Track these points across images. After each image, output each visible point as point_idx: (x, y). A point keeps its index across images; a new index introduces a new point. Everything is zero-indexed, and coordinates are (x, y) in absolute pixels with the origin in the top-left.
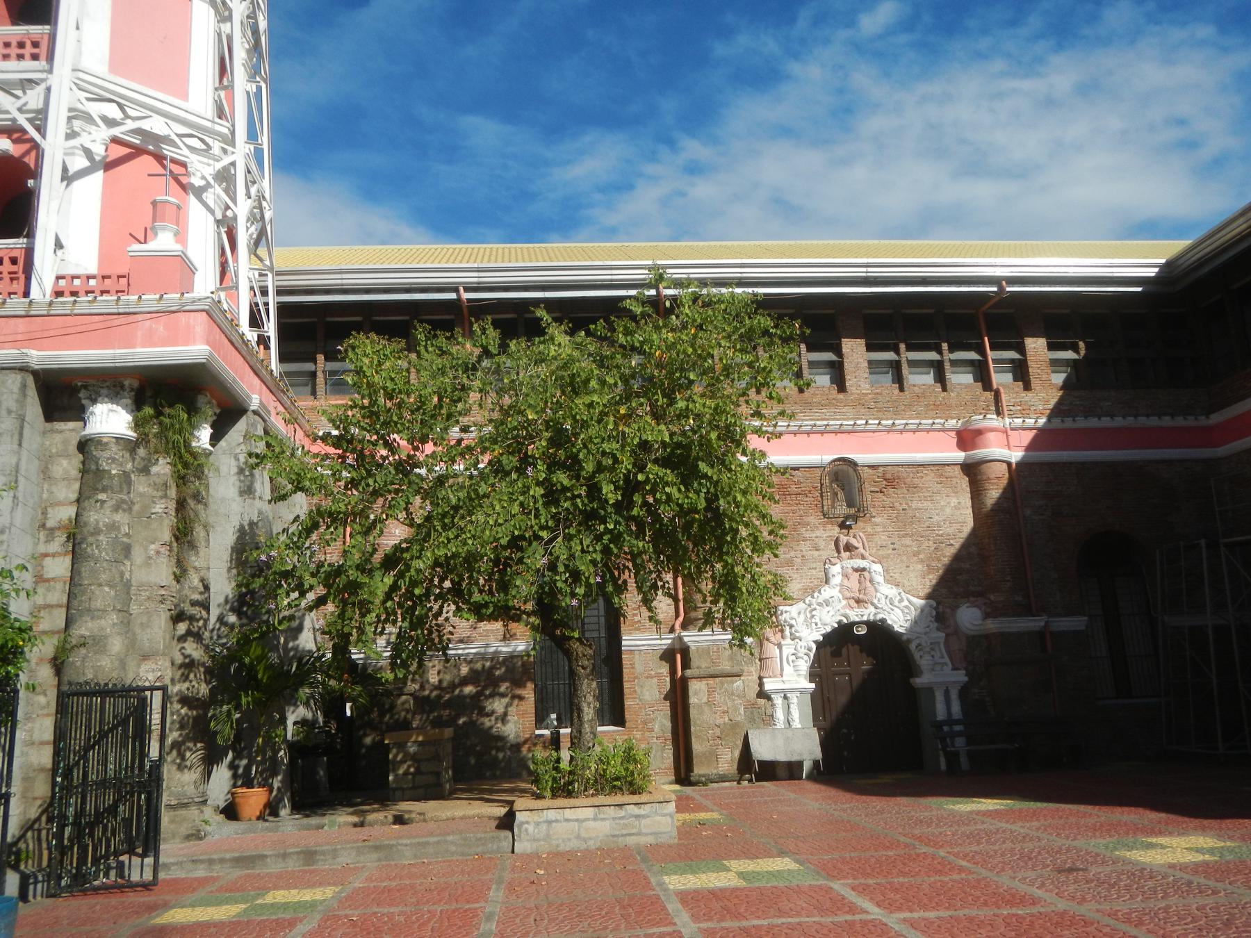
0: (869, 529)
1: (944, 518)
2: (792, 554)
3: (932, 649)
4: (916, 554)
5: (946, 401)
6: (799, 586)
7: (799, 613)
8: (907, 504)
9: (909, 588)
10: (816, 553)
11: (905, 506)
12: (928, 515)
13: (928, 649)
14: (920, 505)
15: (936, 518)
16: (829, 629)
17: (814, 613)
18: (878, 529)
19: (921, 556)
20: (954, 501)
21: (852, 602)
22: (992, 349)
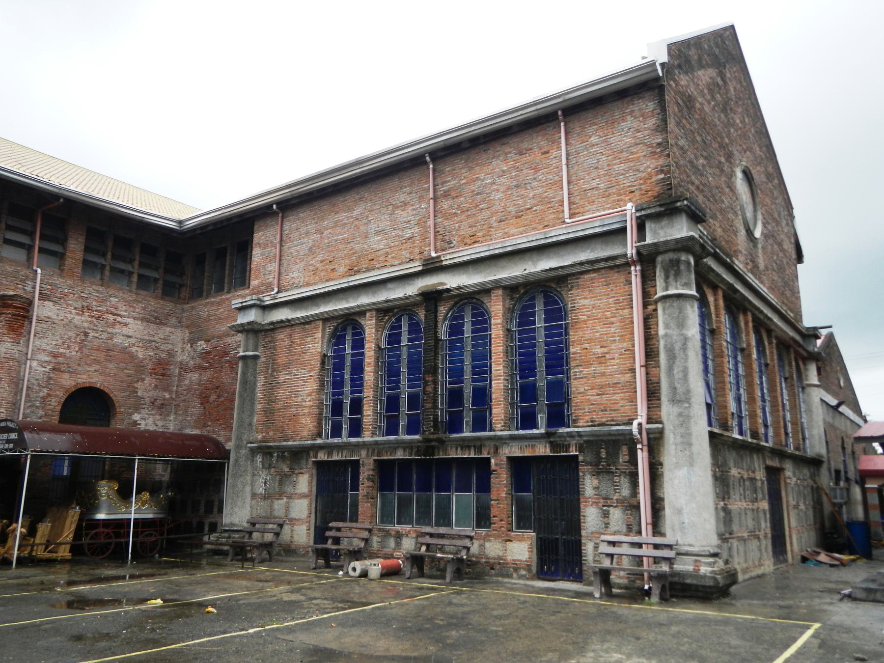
22: (41, 238)
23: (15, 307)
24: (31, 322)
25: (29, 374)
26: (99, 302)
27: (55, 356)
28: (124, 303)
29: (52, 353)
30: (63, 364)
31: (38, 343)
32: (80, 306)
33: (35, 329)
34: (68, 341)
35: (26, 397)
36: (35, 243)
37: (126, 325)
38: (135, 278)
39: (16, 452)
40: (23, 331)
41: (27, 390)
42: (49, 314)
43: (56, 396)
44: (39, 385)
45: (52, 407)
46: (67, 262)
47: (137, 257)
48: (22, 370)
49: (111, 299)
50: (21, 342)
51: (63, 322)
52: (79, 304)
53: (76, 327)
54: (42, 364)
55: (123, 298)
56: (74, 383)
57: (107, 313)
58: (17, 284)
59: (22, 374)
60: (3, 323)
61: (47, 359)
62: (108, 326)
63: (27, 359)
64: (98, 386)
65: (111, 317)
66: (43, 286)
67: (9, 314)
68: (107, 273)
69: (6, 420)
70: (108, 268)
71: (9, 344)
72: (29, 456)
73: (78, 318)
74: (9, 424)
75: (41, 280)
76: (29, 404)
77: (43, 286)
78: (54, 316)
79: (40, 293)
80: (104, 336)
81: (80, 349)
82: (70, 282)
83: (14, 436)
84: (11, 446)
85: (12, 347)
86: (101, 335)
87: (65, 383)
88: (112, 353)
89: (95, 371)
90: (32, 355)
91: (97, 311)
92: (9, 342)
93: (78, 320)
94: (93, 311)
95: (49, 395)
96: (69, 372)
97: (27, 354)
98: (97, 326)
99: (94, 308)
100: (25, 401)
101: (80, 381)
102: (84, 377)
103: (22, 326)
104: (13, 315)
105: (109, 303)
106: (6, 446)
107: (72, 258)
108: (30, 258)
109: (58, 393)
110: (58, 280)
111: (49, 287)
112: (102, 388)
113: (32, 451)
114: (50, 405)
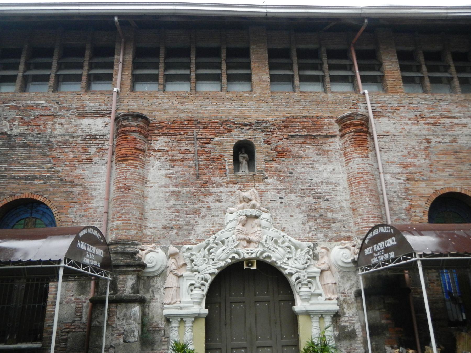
0: (262, 187)
1: (321, 180)
2: (200, 204)
3: (309, 282)
4: (299, 206)
5: (325, 99)
6: (203, 230)
7: (199, 251)
8: (293, 169)
9: (292, 233)
10: (218, 204)
11: (291, 171)
12: (309, 178)
13: (305, 282)
14: (303, 170)
15: (315, 180)
16: (222, 264)
17: (211, 251)
18: (269, 187)
19: (303, 208)
20: (330, 167)
21: (245, 243)
22: (360, 70)
23: (355, 125)
24: (373, 139)
25: (386, 188)
26: (429, 109)
27: (406, 167)
28: (455, 105)
29: (401, 164)
30: (415, 173)
31: (385, 156)
32: (413, 116)
33: (379, 144)
34: (413, 150)
35: (390, 210)
36: (356, 72)
37: (465, 125)
38: (456, 82)
39: (400, 261)
40: (368, 146)
41: (389, 204)
42: (387, 129)
43: (419, 206)
44: (399, 197)
45: (419, 218)
46: (388, 81)
47: (451, 63)
48: (378, 184)
49: (441, 103)
50: (369, 155)
51: (402, 134)
52: (412, 115)
53: (416, 135)
54: (396, 176)
55: (453, 101)
56: (433, 191)
57: (442, 117)
58: (350, 108)
59: (379, 189)
60: (349, 142)
61: (399, 170)
62: (447, 130)
63: (380, 173)
64: (459, 190)
65: (448, 121)
66: (374, 105)
67: (351, 132)
68: (427, 83)
69: (377, 227)
70: (427, 79)
71: (359, 160)
72: (419, 263)
73: (414, 127)
74: (382, 230)
75: (371, 100)
76: (395, 217)
77: (374, 105)
78: (392, 130)
79: (374, 112)
80: (447, 139)
81: (427, 156)
82: (396, 96)
83: (391, 242)
84: (392, 255)
85: (363, 162)
86: (443, 139)
87: (423, 192)
88: (461, 155)
89: (450, 175)
90: (383, 169)
91: (431, 117)
92: (359, 157)
93: (415, 129)
94: (427, 118)
95: (412, 206)
96: (424, 180)
97: (378, 169)
98: (436, 132)
99: (428, 115)
100: (391, 215)
101: (438, 188)
102: (441, 183)
103: (366, 141)
104: (355, 132)
105: (440, 108)
106: (386, 256)
107: (391, 77)
108: (356, 89)
109: (419, 202)
110: (384, 97)
111: (379, 105)
112: (463, 192)
113: (421, 256)
114: (415, 216)
